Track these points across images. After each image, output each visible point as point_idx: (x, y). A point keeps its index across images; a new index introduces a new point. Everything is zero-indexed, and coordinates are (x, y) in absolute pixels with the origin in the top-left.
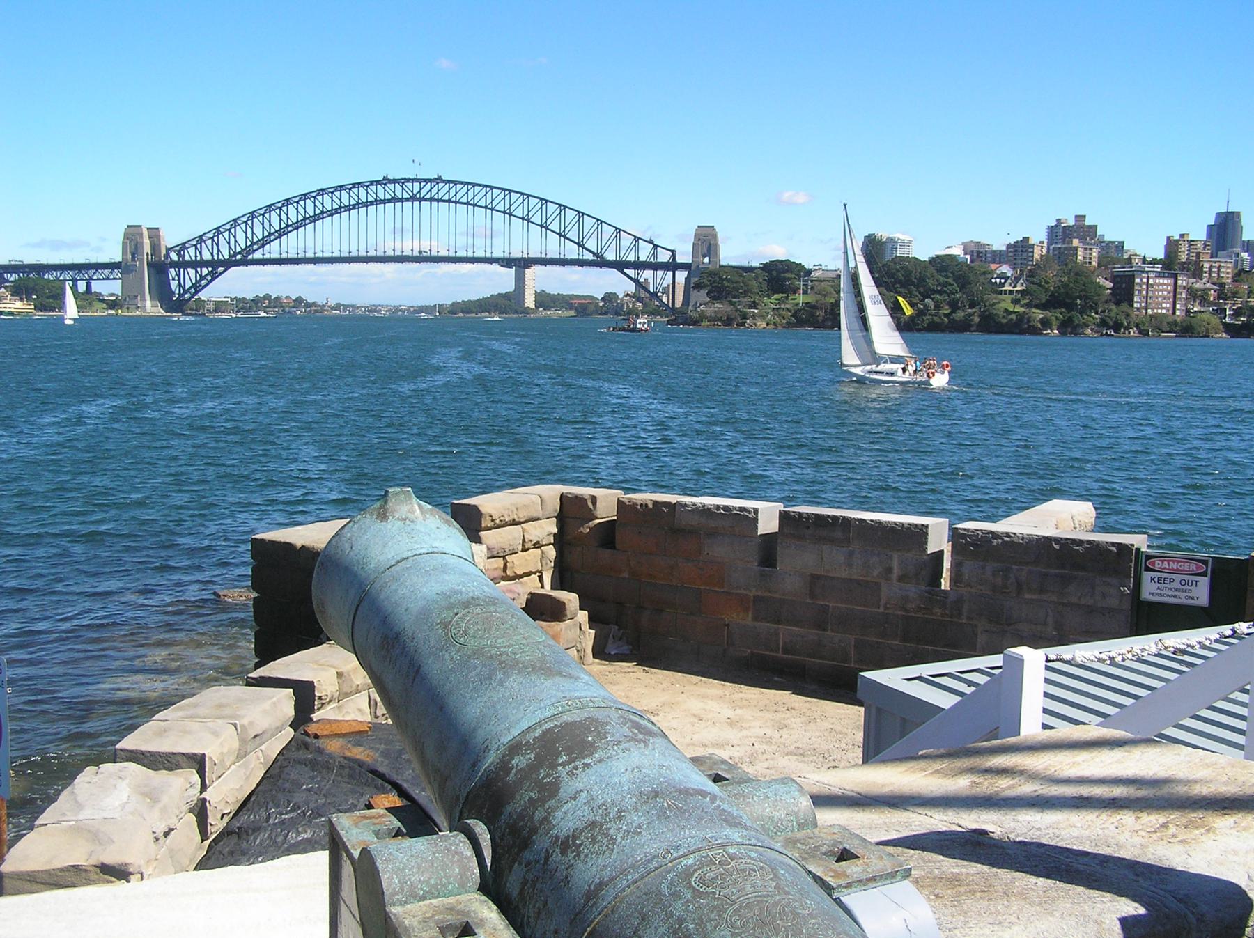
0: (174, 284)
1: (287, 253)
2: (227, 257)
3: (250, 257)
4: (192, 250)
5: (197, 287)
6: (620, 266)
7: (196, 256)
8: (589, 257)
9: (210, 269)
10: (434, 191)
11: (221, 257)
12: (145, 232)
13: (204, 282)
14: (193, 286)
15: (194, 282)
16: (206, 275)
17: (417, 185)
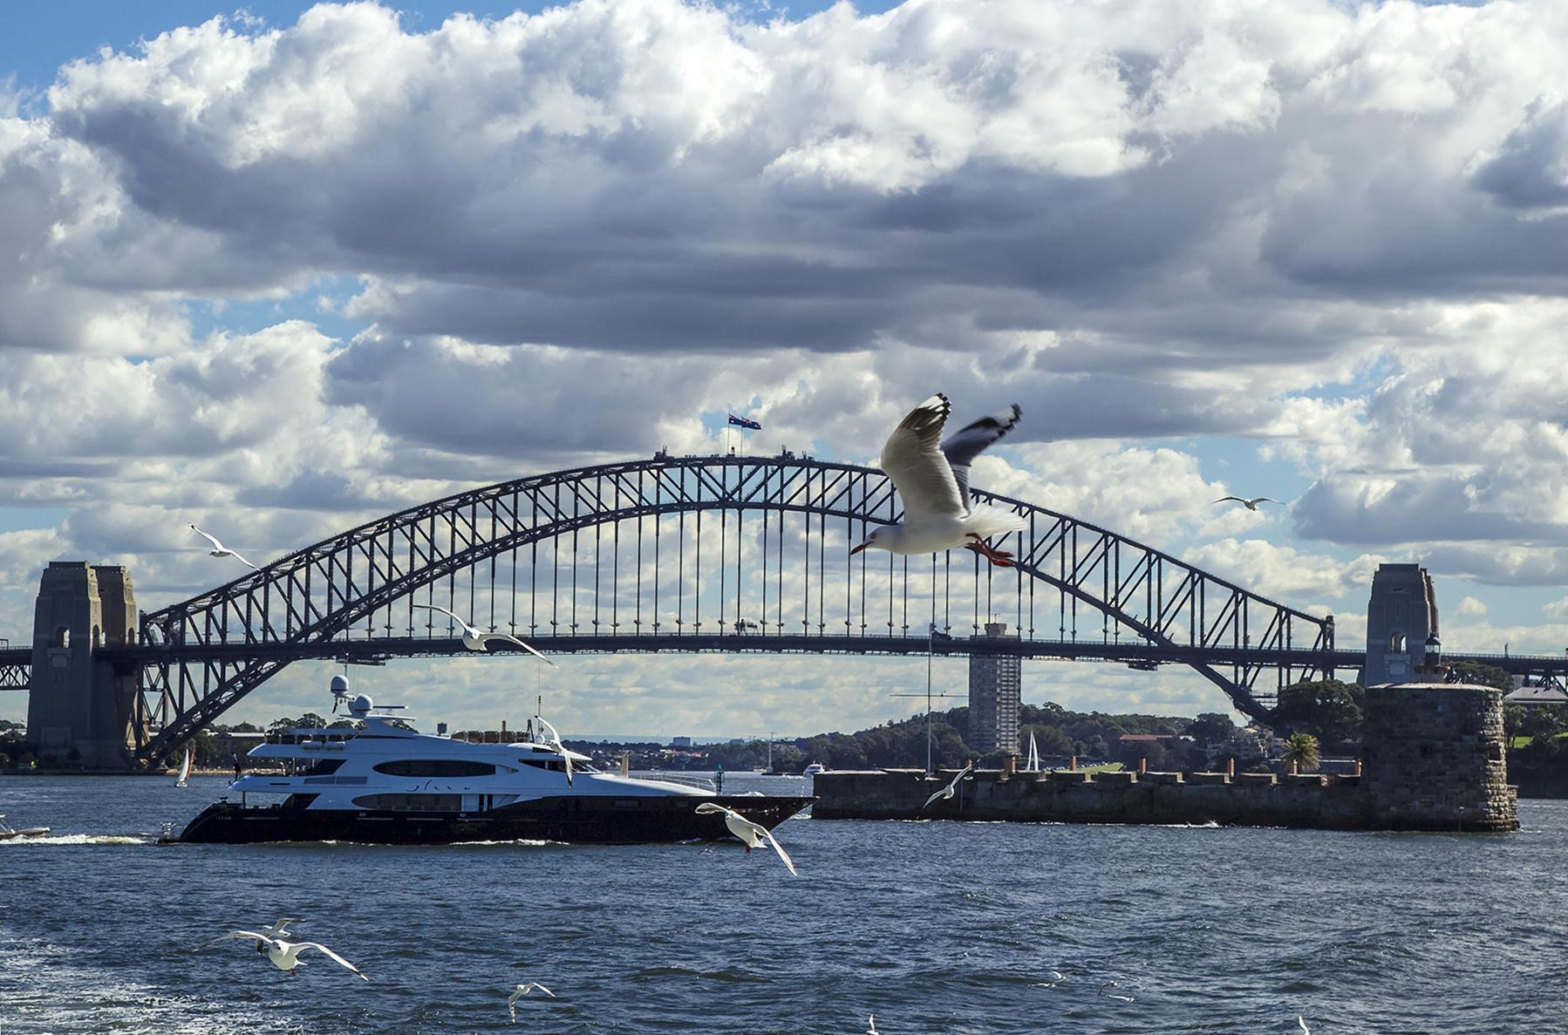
0: (153, 700)
1: (388, 627)
2: (282, 637)
3: (340, 636)
4: (200, 619)
5: (211, 706)
6: (1200, 657)
7: (208, 634)
8: (1128, 636)
9: (242, 666)
10: (774, 484)
11: (270, 638)
12: (92, 578)
13: (228, 694)
14: (199, 706)
15: (201, 697)
16: (234, 680)
17: (732, 470)
